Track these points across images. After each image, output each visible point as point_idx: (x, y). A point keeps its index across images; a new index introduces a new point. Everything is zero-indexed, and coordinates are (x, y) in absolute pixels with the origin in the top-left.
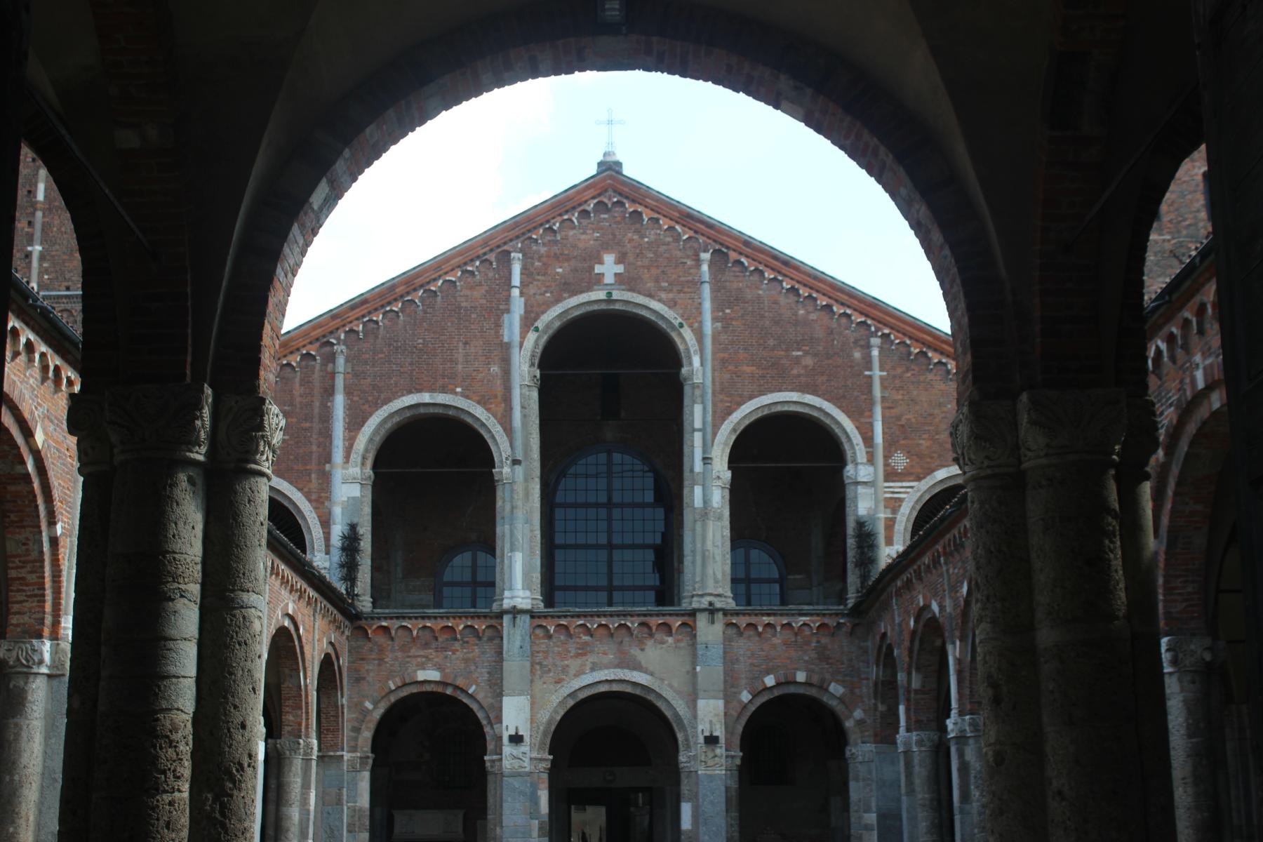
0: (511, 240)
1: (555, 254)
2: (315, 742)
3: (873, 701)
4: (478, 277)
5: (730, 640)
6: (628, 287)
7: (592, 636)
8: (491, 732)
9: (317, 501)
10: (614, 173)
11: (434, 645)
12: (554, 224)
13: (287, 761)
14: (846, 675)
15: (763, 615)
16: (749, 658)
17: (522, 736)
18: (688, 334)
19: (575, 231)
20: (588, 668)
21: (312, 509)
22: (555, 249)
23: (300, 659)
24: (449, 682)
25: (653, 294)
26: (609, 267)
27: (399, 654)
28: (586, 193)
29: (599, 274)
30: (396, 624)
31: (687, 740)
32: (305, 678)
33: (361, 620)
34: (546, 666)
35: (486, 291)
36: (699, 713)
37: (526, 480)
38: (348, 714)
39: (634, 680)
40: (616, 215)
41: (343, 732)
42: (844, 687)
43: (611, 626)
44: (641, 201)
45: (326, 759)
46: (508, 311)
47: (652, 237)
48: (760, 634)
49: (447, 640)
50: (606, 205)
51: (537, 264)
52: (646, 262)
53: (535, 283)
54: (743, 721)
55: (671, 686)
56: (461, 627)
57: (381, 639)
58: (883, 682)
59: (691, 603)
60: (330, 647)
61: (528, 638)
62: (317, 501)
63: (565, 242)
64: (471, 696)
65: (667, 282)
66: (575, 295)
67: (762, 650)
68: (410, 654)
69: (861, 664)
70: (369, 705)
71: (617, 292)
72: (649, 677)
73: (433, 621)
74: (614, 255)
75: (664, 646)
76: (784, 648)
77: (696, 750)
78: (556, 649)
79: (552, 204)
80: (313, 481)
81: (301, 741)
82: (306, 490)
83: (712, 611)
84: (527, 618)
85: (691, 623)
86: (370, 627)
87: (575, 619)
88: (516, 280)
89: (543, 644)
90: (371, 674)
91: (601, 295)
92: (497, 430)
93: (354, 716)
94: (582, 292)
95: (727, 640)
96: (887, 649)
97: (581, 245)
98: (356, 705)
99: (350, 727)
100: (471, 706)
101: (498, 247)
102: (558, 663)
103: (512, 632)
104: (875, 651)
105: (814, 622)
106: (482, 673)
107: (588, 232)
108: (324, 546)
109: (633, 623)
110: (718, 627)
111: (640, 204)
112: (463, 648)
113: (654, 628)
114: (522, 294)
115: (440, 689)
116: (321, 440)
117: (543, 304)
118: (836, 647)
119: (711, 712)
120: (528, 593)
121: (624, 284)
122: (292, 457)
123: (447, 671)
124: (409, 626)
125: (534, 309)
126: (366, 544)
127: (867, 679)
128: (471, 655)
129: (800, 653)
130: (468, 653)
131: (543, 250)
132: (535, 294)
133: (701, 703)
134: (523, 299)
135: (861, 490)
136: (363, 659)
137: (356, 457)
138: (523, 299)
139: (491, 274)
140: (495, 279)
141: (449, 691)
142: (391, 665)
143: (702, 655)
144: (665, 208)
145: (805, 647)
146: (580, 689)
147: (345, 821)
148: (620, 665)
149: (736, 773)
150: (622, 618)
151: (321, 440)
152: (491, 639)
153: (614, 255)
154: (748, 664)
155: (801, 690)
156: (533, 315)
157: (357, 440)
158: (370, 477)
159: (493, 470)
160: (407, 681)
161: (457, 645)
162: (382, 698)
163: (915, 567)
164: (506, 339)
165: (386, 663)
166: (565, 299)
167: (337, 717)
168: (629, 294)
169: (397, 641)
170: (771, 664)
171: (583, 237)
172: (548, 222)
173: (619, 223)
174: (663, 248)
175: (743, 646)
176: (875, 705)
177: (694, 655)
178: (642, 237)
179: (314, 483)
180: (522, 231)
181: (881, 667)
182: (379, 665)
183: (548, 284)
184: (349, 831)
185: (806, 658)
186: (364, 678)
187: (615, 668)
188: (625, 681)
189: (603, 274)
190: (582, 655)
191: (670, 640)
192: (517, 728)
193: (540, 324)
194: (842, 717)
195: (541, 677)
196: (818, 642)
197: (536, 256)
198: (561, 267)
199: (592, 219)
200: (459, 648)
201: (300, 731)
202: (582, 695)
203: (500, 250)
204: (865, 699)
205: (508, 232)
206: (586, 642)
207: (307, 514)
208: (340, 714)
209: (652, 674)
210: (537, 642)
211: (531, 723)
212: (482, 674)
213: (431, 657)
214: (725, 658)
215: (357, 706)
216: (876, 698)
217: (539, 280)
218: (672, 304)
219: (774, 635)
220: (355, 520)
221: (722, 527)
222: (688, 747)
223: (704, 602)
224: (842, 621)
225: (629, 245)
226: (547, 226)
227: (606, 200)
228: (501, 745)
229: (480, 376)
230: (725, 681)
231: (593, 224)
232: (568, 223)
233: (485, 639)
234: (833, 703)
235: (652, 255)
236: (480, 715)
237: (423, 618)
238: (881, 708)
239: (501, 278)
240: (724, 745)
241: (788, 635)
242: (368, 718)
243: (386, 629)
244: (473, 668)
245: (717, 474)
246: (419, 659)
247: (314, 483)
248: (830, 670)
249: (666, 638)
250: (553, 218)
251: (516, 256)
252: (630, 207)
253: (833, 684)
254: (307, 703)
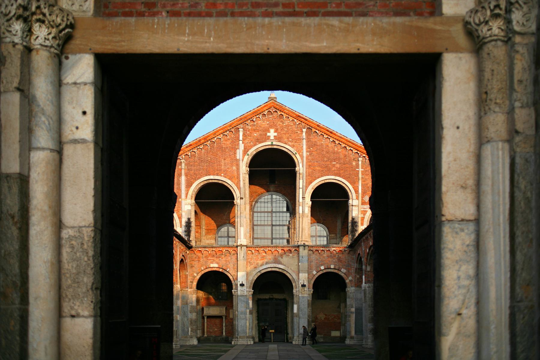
0: (239, 124)
1: (254, 129)
3: (355, 274)
4: (228, 137)
5: (310, 255)
6: (278, 141)
7: (266, 253)
8: (234, 283)
10: (274, 101)
11: (216, 256)
12: (254, 119)
14: (347, 266)
15: (321, 247)
16: (316, 261)
17: (244, 284)
18: (298, 156)
19: (261, 121)
20: (265, 263)
22: (254, 127)
25: (286, 142)
26: (272, 134)
27: (205, 259)
28: (264, 108)
29: (269, 136)
30: (204, 249)
31: (296, 286)
34: (251, 263)
35: (231, 142)
36: (300, 277)
37: (245, 204)
39: (279, 267)
40: (274, 116)
42: (346, 270)
43: (272, 251)
44: (283, 111)
46: (238, 148)
47: (287, 124)
48: (319, 253)
49: (220, 255)
50: (271, 112)
51: (248, 132)
52: (284, 132)
53: (247, 139)
54: (314, 280)
55: (291, 269)
57: (199, 254)
58: (358, 268)
59: (298, 244)
60: (183, 256)
61: (245, 254)
63: (257, 125)
64: (228, 272)
65: (291, 139)
66: (261, 143)
67: (320, 258)
68: (208, 259)
69: (352, 263)
70: (195, 275)
71: (275, 142)
72: (284, 266)
73: (215, 248)
74: (273, 130)
75: (289, 257)
76: (327, 258)
77: (299, 288)
78: (254, 257)
79: (253, 112)
83: (304, 246)
84: (245, 248)
85: (298, 250)
86: (195, 250)
87: (261, 248)
88: (241, 138)
89: (250, 256)
90: (196, 265)
91: (270, 143)
92: (235, 188)
93: (191, 278)
94: (263, 142)
95: (309, 255)
96: (360, 258)
97: (263, 126)
99: (190, 281)
101: (235, 126)
102: (255, 262)
103: (240, 252)
104: (356, 259)
105: (337, 250)
107: (265, 121)
108: (180, 225)
109: (279, 250)
110: (306, 251)
111: (282, 112)
112: (225, 257)
113: (286, 251)
114: (243, 143)
115: (218, 269)
117: (250, 146)
118: (344, 257)
119: (303, 277)
120: (245, 240)
121: (277, 140)
123: (220, 264)
124: (208, 250)
125: (247, 148)
127: (354, 267)
128: (227, 259)
129: (332, 259)
130: (227, 259)
131: (250, 128)
132: (247, 143)
133: (300, 274)
134: (243, 145)
135: (354, 208)
136: (193, 260)
138: (243, 145)
139: (233, 136)
140: (234, 138)
141: (221, 270)
142: (202, 262)
143: (301, 260)
144: (291, 114)
145: (334, 258)
146: (262, 270)
148: (275, 263)
149: (311, 296)
150: (276, 248)
152: (234, 254)
153: (273, 130)
154: (315, 262)
155: (332, 271)
156: (247, 150)
159: (234, 201)
160: (207, 267)
161: (223, 256)
163: (369, 233)
164: (238, 158)
165: (201, 261)
166: (257, 144)
168: (279, 143)
169: (204, 255)
170: (323, 262)
171: (264, 123)
172: (252, 118)
173: (276, 119)
174: (290, 127)
175: (314, 257)
176: (356, 275)
177: (299, 260)
178: (283, 123)
180: (243, 121)
181: (358, 264)
182: (198, 262)
183: (252, 139)
185: (334, 261)
186: (194, 266)
187: (273, 263)
188: (276, 267)
189: (270, 136)
190: (263, 259)
191: (291, 255)
192: (242, 282)
193: (249, 153)
194: (345, 279)
195: (250, 266)
196: (338, 256)
197: (248, 130)
198: (256, 134)
199: (266, 117)
200: (224, 257)
202: (263, 272)
203: (235, 128)
204: (353, 274)
205: (238, 121)
206: (264, 256)
209: (285, 266)
210: (249, 255)
211: (247, 280)
212: (231, 265)
213: (215, 260)
214: (308, 261)
215: (192, 275)
216: (356, 273)
217: (249, 138)
218: (293, 146)
219: (324, 254)
220: (190, 217)
222: (296, 288)
223: (302, 243)
224: (346, 249)
225: (279, 126)
226: (251, 120)
227: (271, 111)
228: (237, 287)
229: (229, 170)
230: (308, 268)
231: (267, 119)
232: (259, 118)
234: (343, 275)
235: (286, 130)
238: (358, 276)
239: (236, 137)
241: (329, 253)
246: (211, 261)
248: (342, 265)
249: (290, 254)
250: (253, 117)
251: (241, 130)
252: (279, 113)
253: (342, 269)
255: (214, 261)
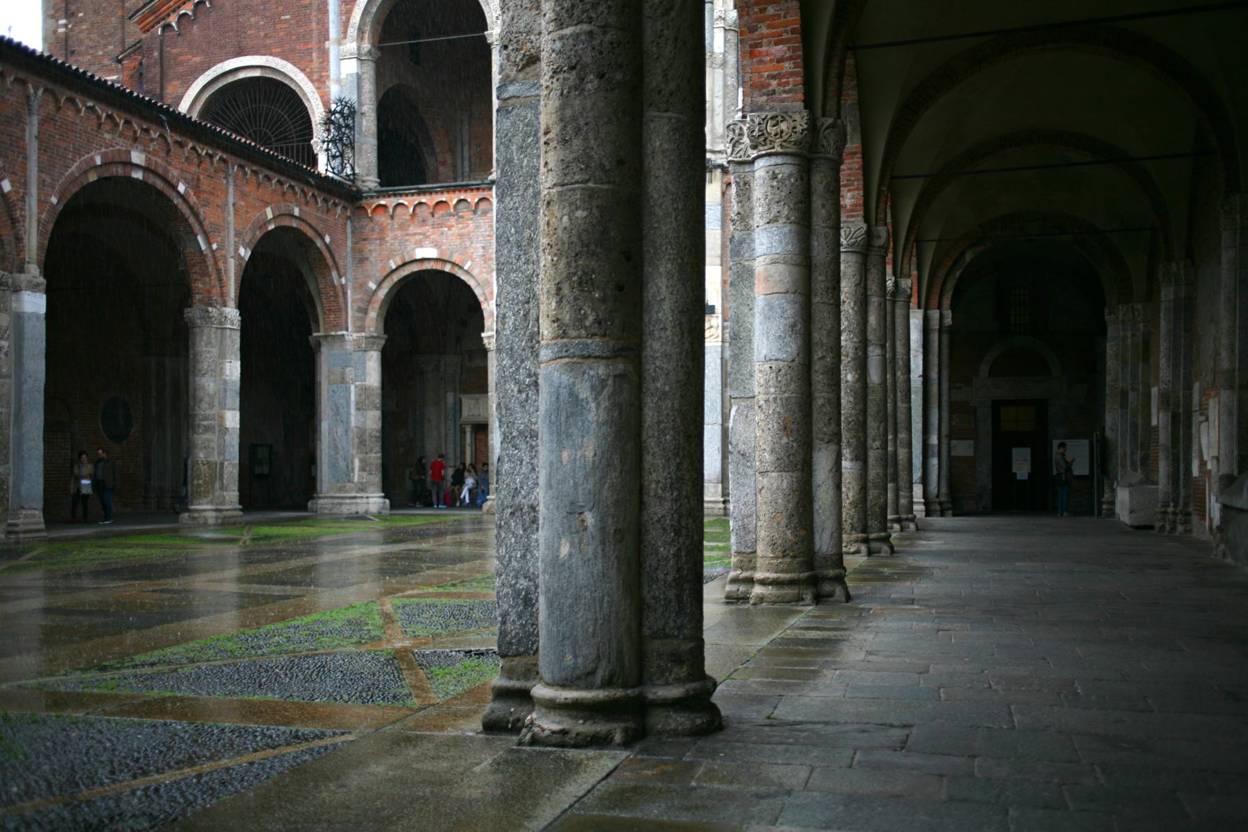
2: (232, 313)
9: (318, 80)
13: (197, 330)
21: (314, 90)
23: (192, 220)
24: (446, 258)
27: (399, 233)
32: (209, 243)
33: (361, 198)
38: (352, 295)
41: (347, 313)
45: (329, 339)
49: (443, 215)
56: (455, 201)
57: (381, 218)
62: (318, 80)
64: (467, 272)
70: (373, 286)
73: (428, 197)
80: (315, 60)
81: (210, 309)
82: (308, 70)
90: (374, 254)
98: (361, 285)
100: (469, 283)
106: (476, 248)
115: (438, 266)
116: (320, 16)
122: (294, 37)
123: (444, 247)
124: (406, 203)
126: (368, 124)
128: (465, 231)
130: (464, 228)
136: (364, 240)
137: (352, 32)
141: (447, 268)
142: (392, 245)
147: (353, 398)
151: (320, 16)
157: (353, 14)
158: (370, 52)
160: (407, 259)
161: (452, 221)
162: (386, 277)
167: (336, 296)
169: (396, 219)
179: (315, 65)
182: (381, 245)
184: (358, 409)
201: (210, 298)
207: (310, 95)
208: (341, 294)
215: (362, 286)
221: (725, 76)
233: (479, 213)
236: (478, 291)
237: (419, 194)
240: (720, 316)
242: (374, 298)
243: (385, 206)
244: (468, 243)
245: (719, 14)
246: (417, 237)
247: (315, 65)
254: (219, 271)
255: (427, 237)
